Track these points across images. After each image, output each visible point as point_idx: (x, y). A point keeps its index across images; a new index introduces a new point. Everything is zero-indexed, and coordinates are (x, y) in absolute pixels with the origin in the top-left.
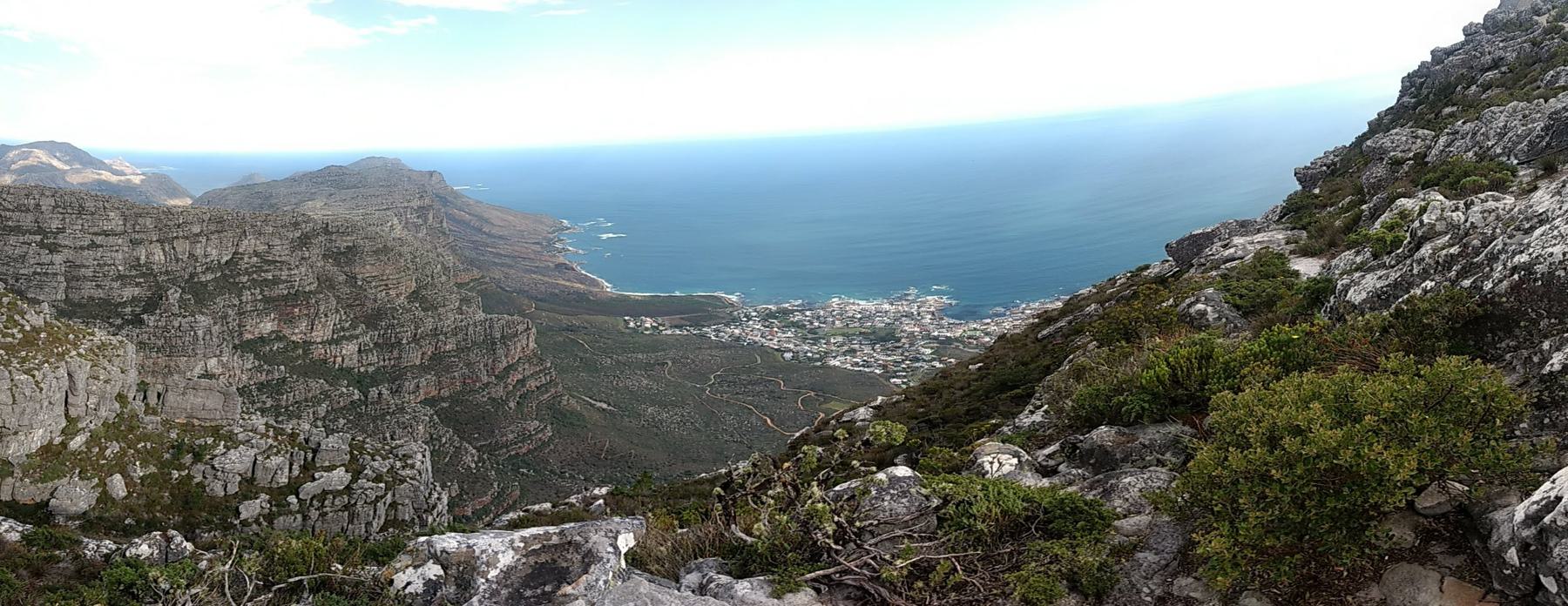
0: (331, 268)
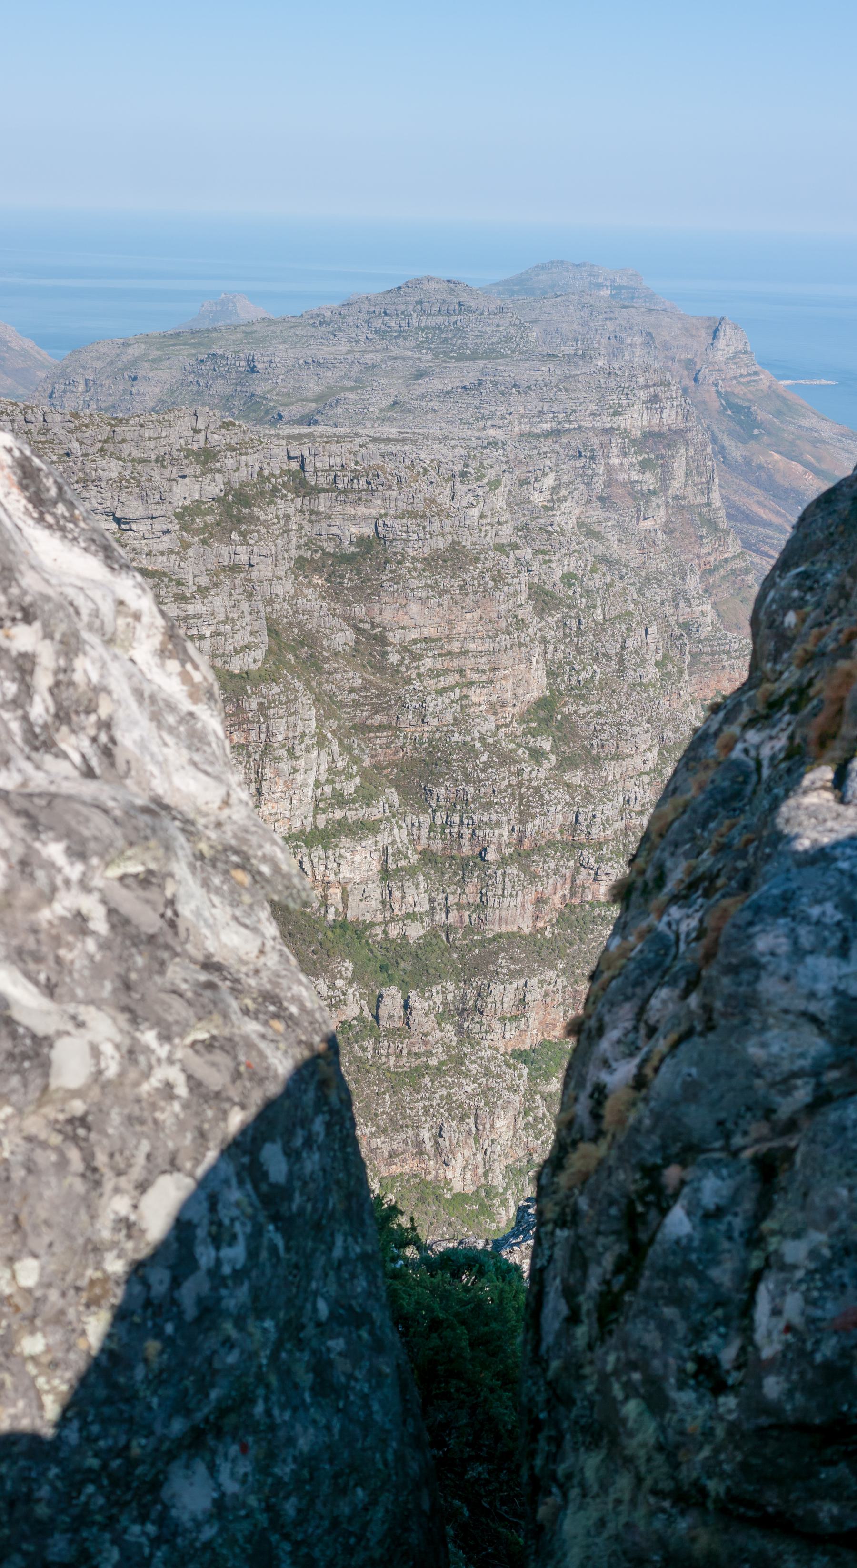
0: (313, 602)
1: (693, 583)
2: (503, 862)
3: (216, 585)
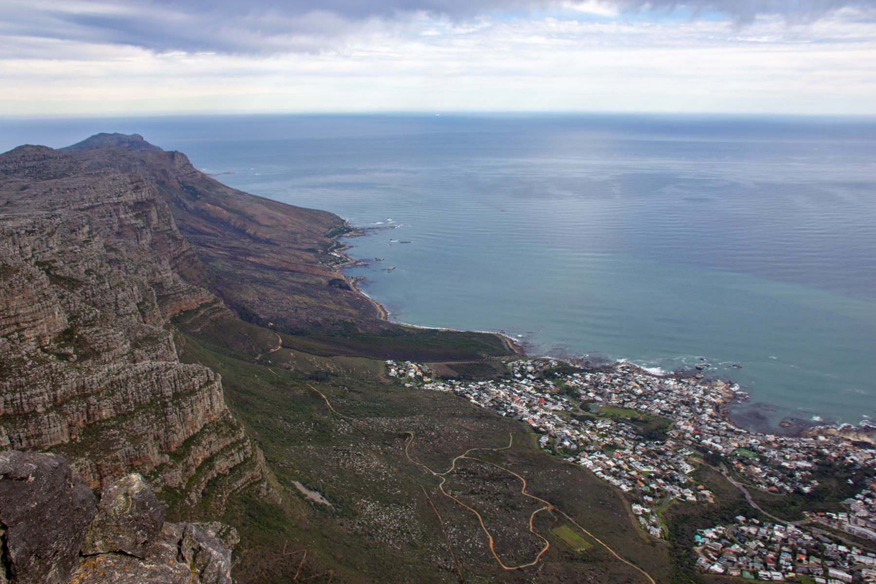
1: (166, 264)
2: (47, 412)
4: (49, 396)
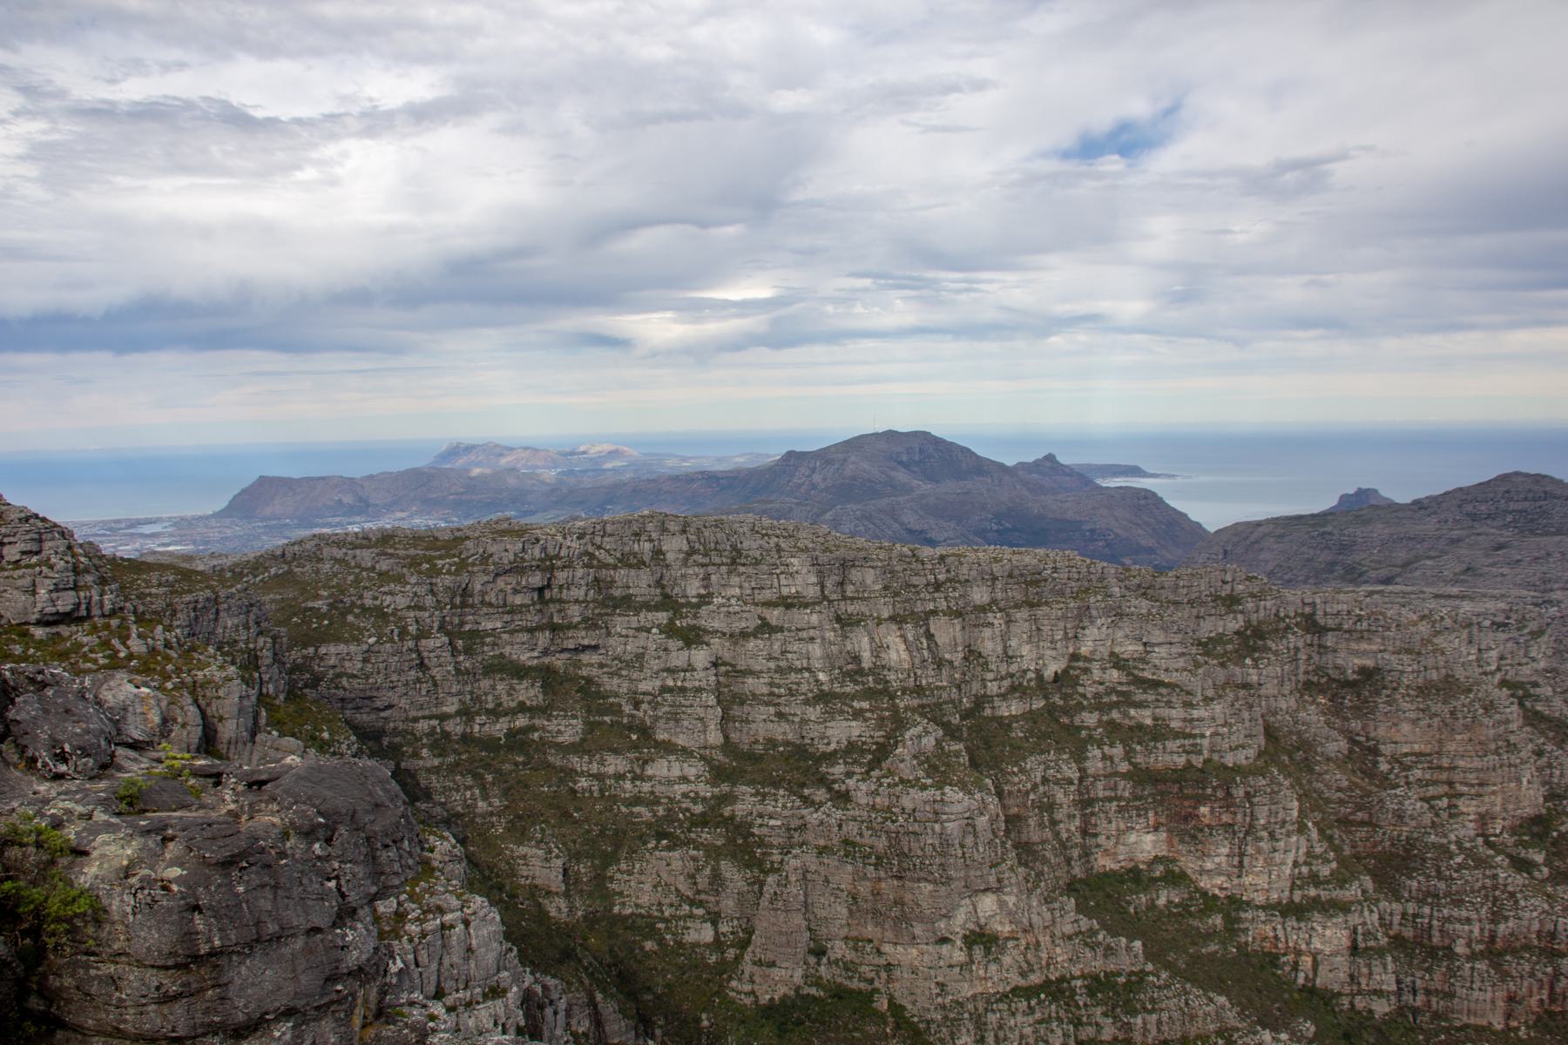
0: (1313, 717)
2: (1473, 957)
3: (1221, 697)
4: (1482, 930)
